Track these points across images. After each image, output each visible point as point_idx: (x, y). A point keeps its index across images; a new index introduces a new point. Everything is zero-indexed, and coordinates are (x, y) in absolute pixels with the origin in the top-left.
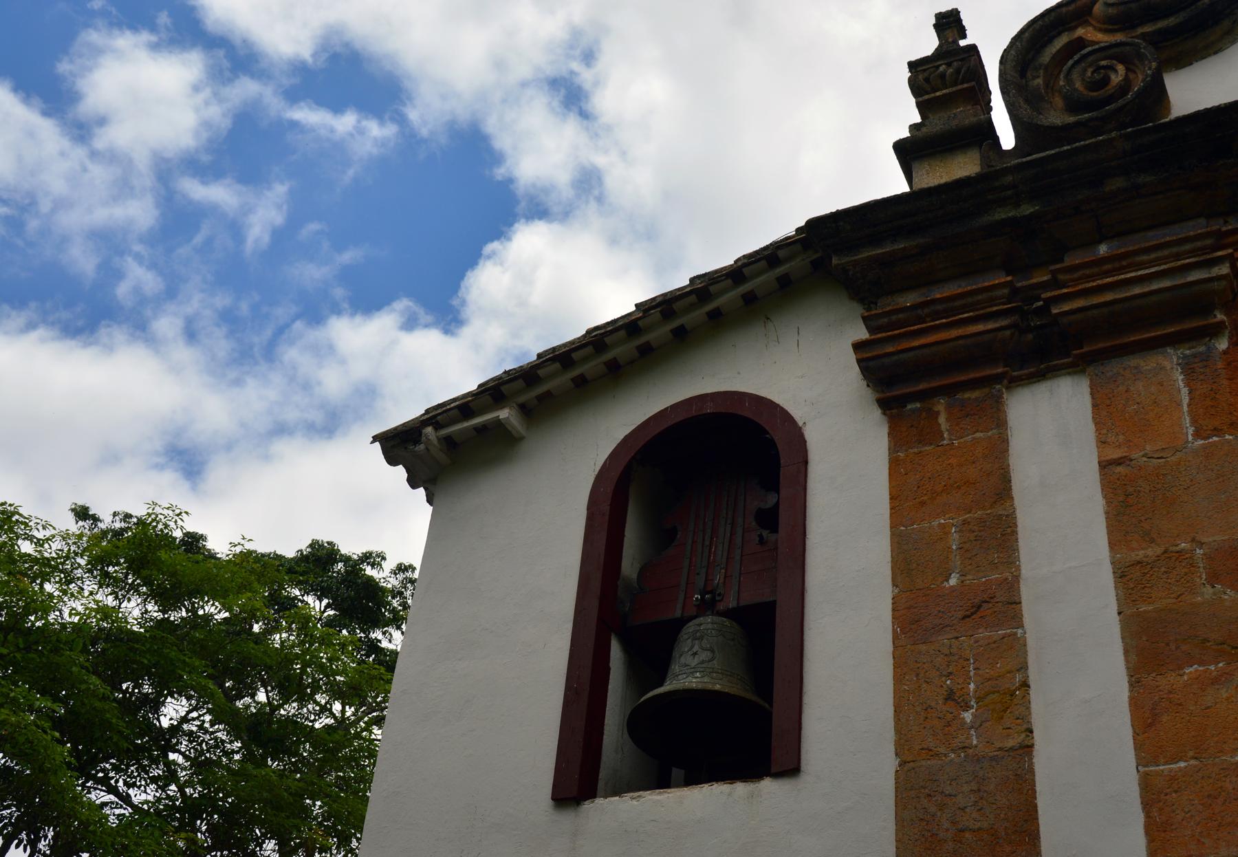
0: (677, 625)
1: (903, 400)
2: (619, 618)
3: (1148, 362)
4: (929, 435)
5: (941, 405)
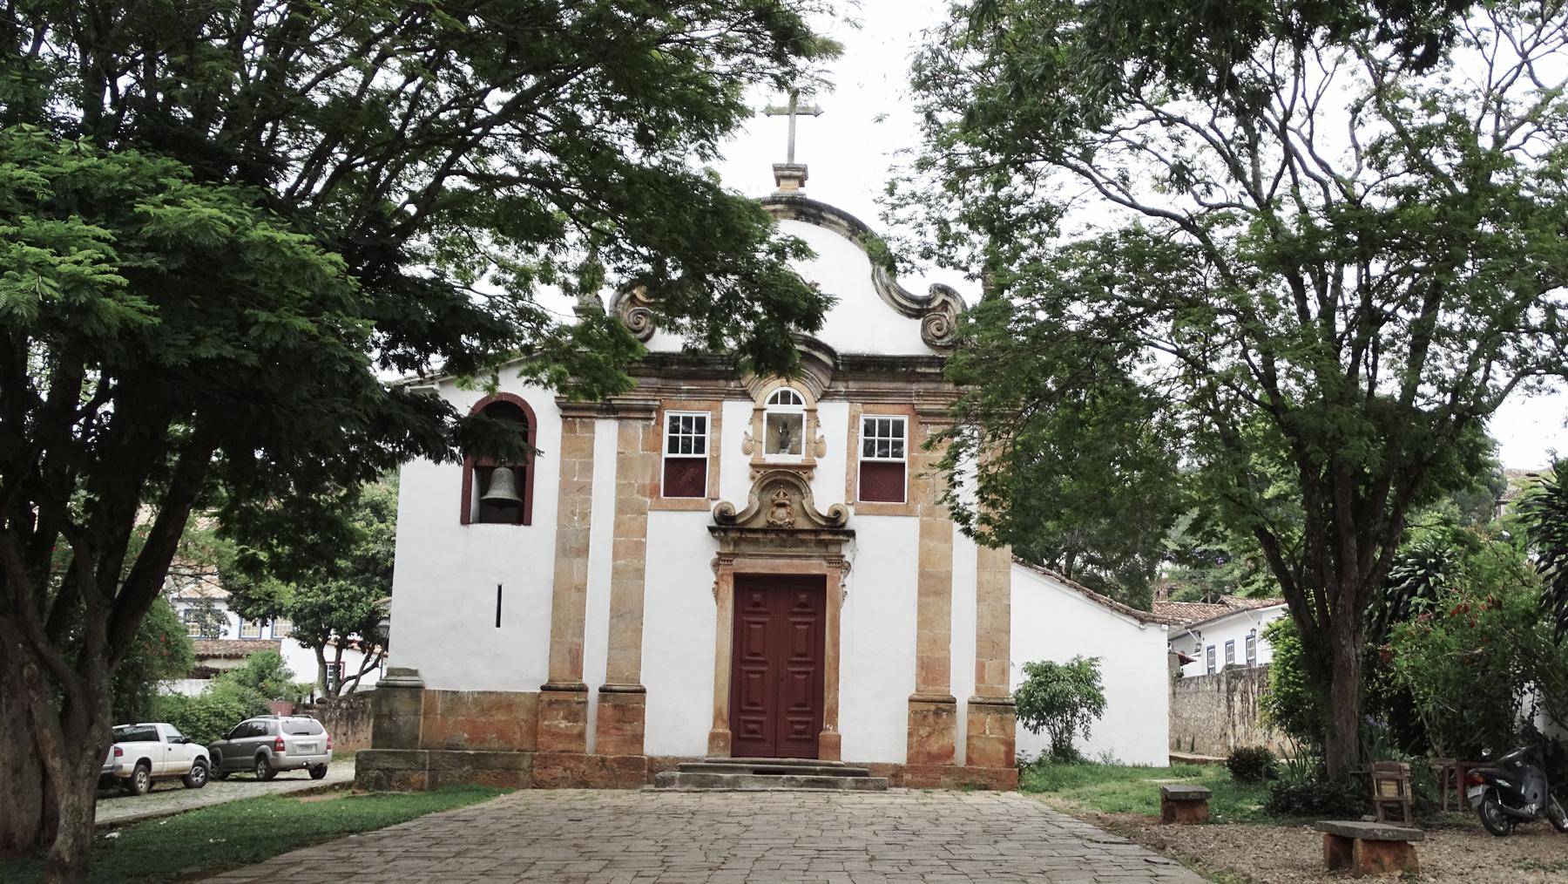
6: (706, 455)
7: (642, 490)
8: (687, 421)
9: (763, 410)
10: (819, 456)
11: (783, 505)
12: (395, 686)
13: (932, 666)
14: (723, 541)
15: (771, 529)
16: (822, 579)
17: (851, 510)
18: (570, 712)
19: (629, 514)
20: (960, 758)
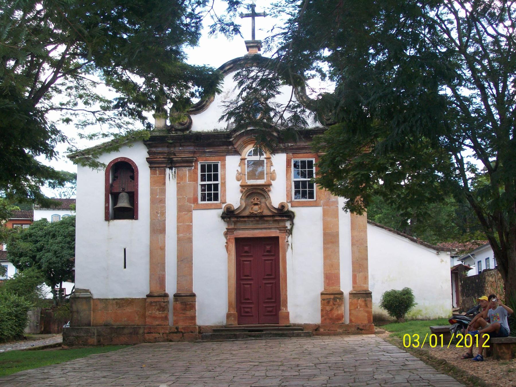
0: (119, 193)
1: (152, 167)
2: (112, 193)
3: (184, 169)
4: (155, 174)
5: (157, 169)
6: (219, 182)
7: (189, 200)
8: (209, 166)
9: (245, 159)
10: (274, 180)
11: (256, 204)
12: (79, 298)
13: (331, 277)
14: (228, 223)
15: (252, 216)
16: (275, 240)
17: (289, 205)
18: (161, 307)
19: (184, 211)
20: (347, 320)
